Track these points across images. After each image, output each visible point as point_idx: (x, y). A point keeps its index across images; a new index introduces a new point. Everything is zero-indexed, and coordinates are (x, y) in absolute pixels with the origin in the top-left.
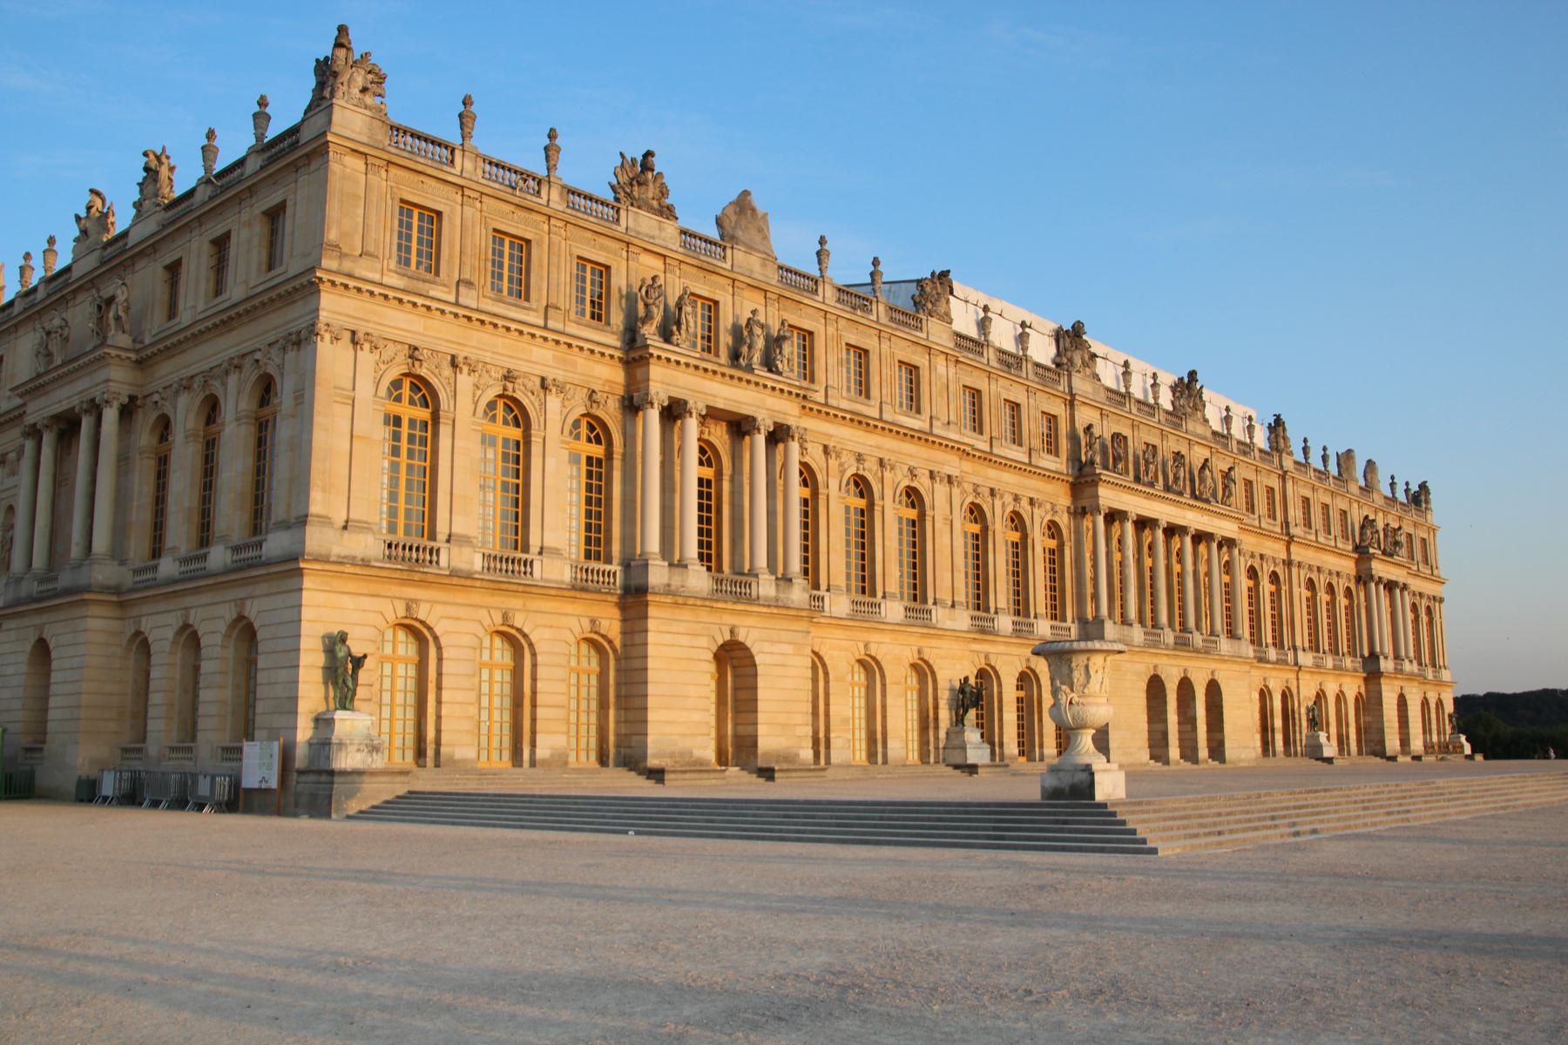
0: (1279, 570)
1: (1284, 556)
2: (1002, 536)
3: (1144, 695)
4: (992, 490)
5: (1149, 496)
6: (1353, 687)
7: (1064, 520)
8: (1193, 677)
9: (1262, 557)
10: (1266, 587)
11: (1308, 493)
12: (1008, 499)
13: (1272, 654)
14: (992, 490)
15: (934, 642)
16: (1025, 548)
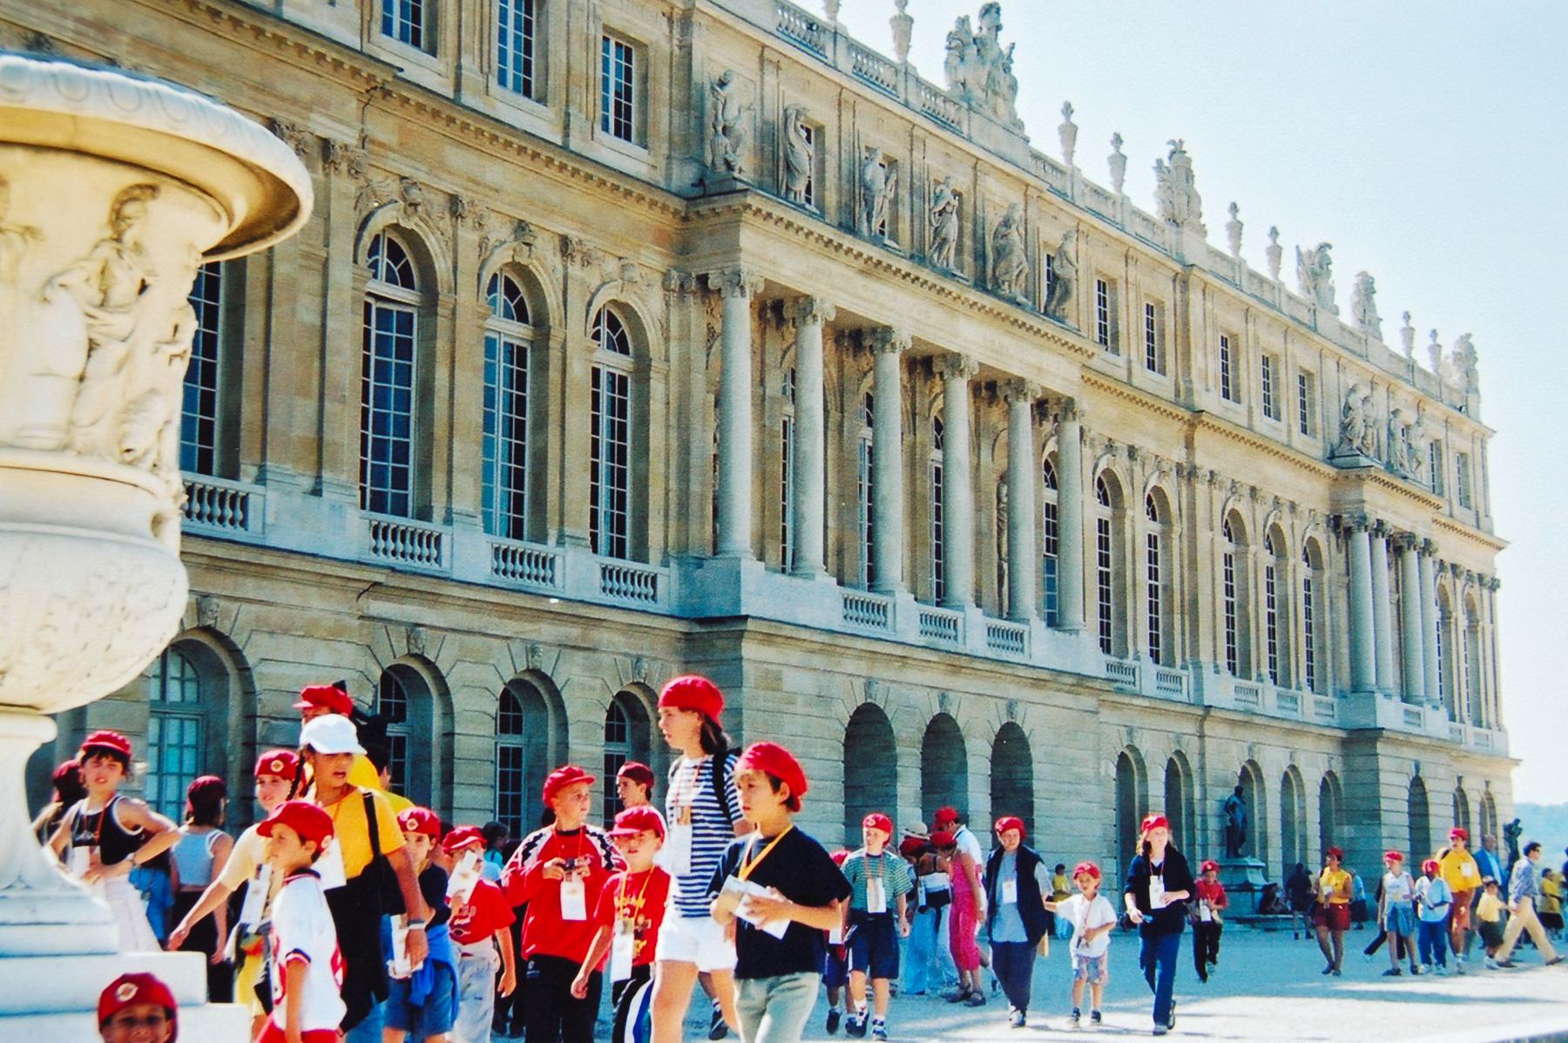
0: (1170, 486)
1: (1178, 454)
2: (475, 325)
3: (838, 754)
4: (454, 200)
5: (873, 269)
6: (1316, 762)
7: (650, 306)
8: (963, 715)
9: (1132, 452)
10: (1139, 524)
11: (1235, 323)
12: (499, 230)
13: (1148, 672)
14: (454, 200)
15: (249, 587)
16: (542, 367)
